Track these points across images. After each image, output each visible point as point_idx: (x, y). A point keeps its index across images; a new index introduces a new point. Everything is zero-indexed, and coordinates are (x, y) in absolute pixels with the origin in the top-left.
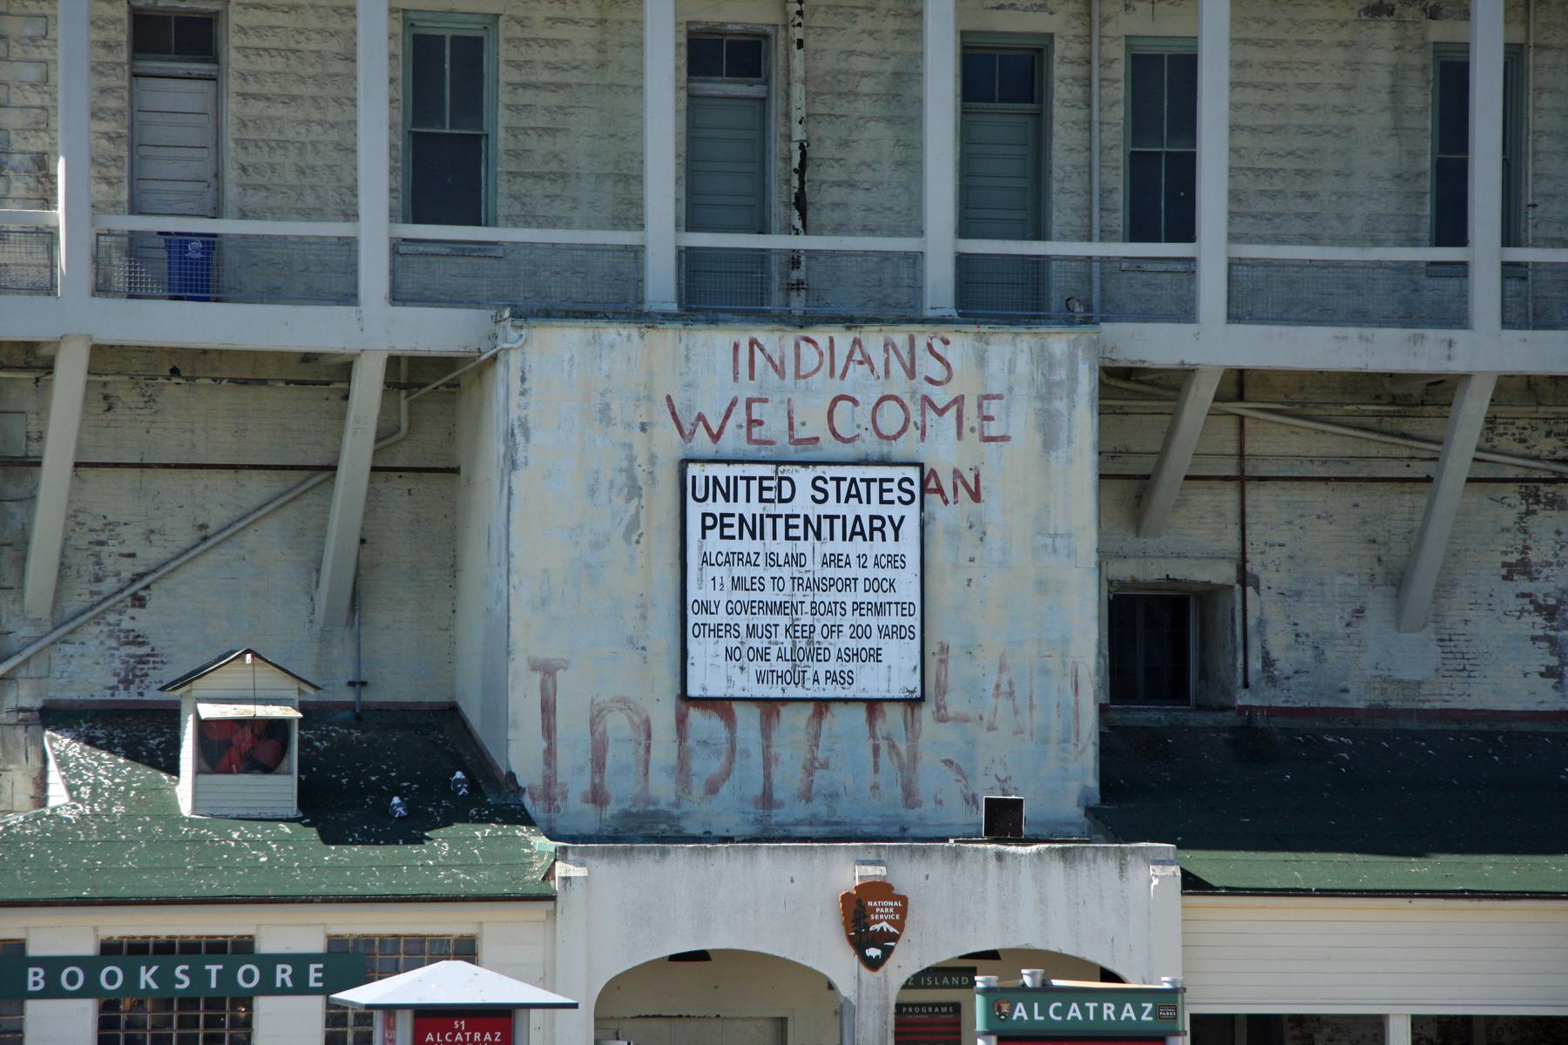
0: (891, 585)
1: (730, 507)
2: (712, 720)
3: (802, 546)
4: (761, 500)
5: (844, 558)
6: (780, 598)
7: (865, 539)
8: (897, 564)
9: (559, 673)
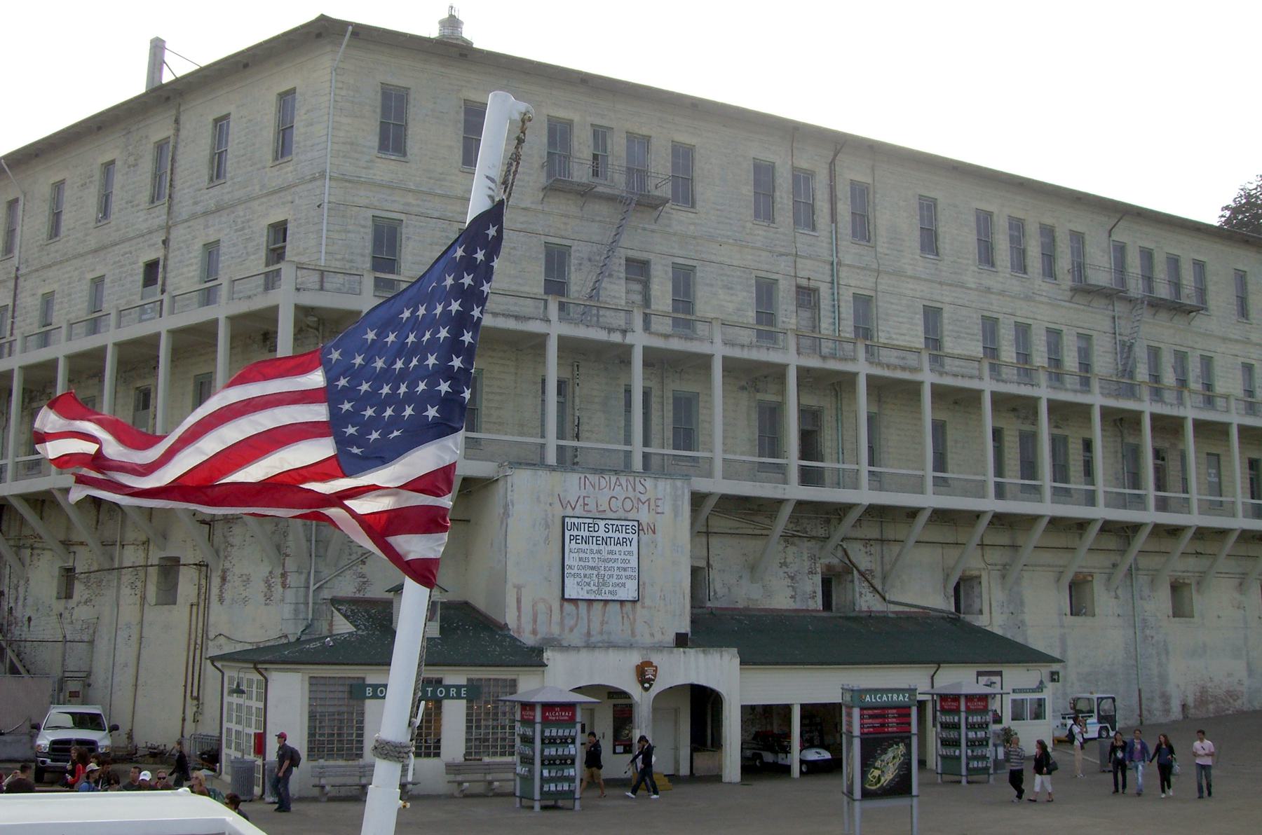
3: (601, 547)
9: (523, 589)
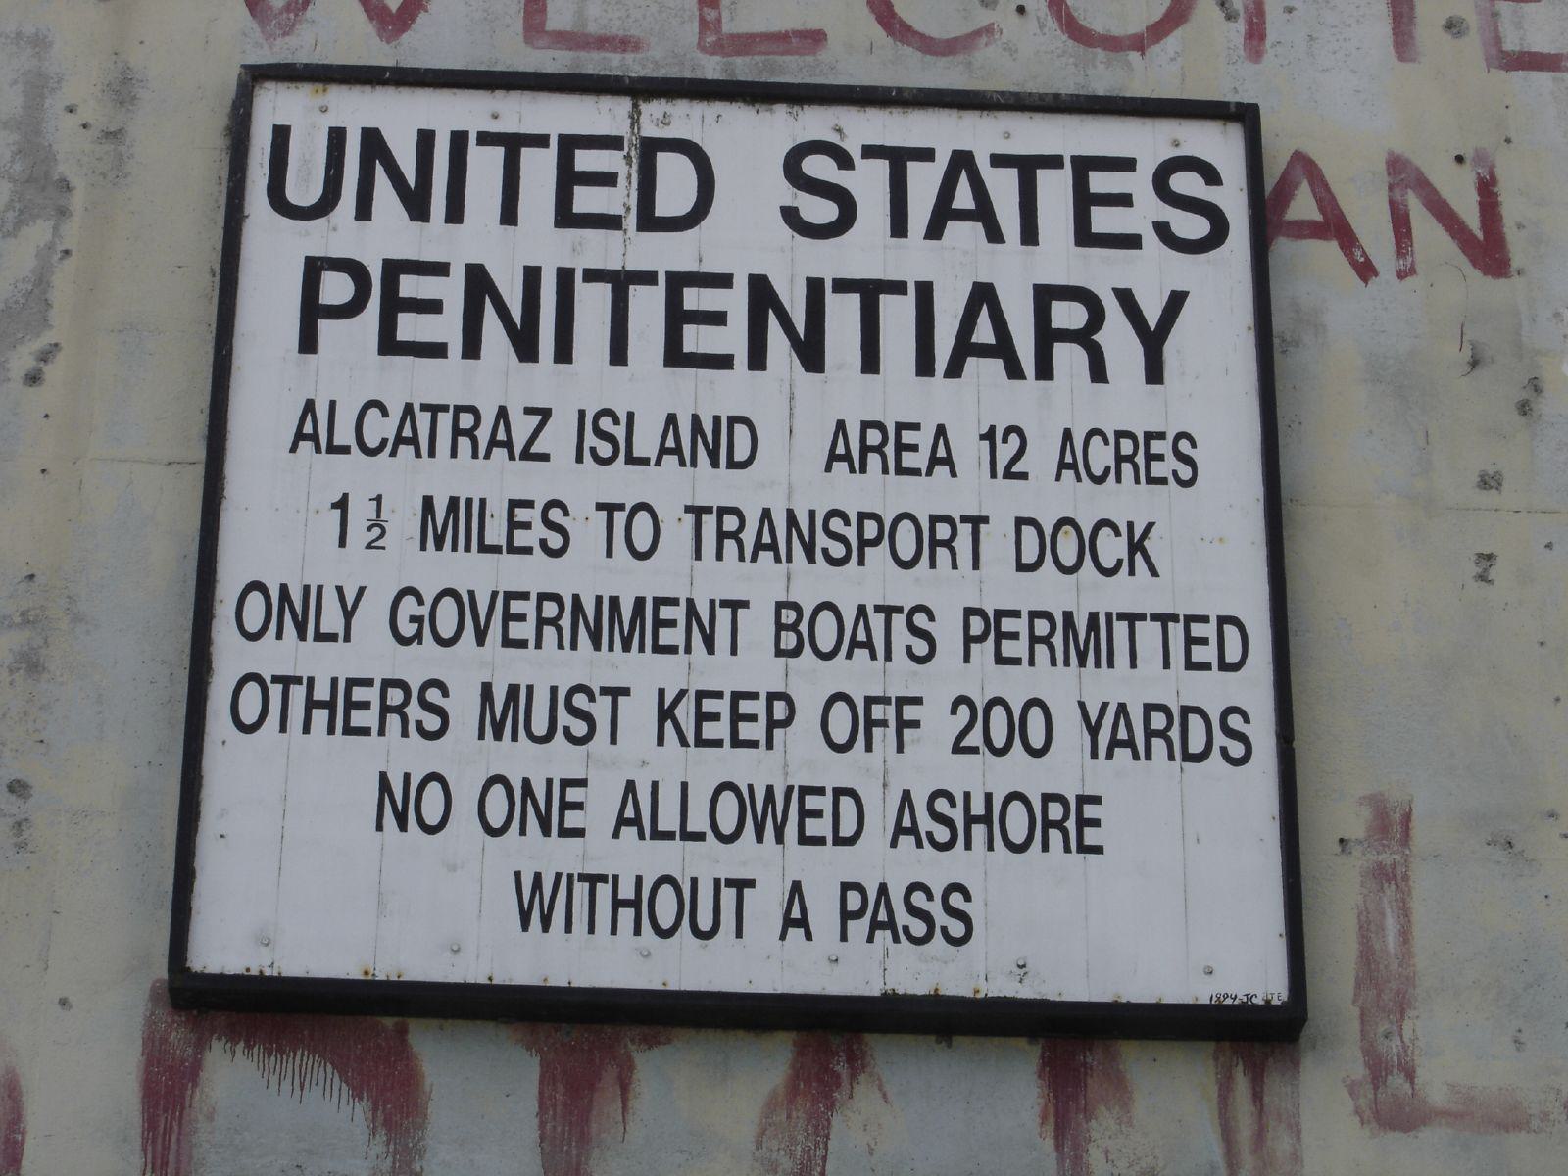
0: (1136, 547)
1: (431, 240)
2: (313, 1094)
4: (566, 217)
5: (924, 438)
6: (629, 581)
7: (1014, 371)
8: (1158, 469)
